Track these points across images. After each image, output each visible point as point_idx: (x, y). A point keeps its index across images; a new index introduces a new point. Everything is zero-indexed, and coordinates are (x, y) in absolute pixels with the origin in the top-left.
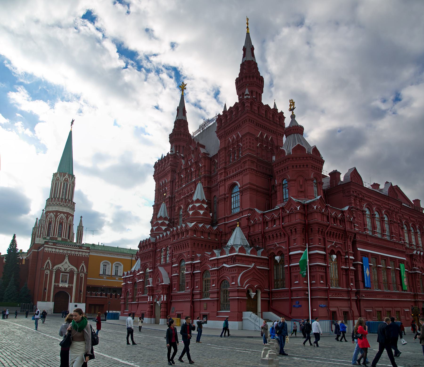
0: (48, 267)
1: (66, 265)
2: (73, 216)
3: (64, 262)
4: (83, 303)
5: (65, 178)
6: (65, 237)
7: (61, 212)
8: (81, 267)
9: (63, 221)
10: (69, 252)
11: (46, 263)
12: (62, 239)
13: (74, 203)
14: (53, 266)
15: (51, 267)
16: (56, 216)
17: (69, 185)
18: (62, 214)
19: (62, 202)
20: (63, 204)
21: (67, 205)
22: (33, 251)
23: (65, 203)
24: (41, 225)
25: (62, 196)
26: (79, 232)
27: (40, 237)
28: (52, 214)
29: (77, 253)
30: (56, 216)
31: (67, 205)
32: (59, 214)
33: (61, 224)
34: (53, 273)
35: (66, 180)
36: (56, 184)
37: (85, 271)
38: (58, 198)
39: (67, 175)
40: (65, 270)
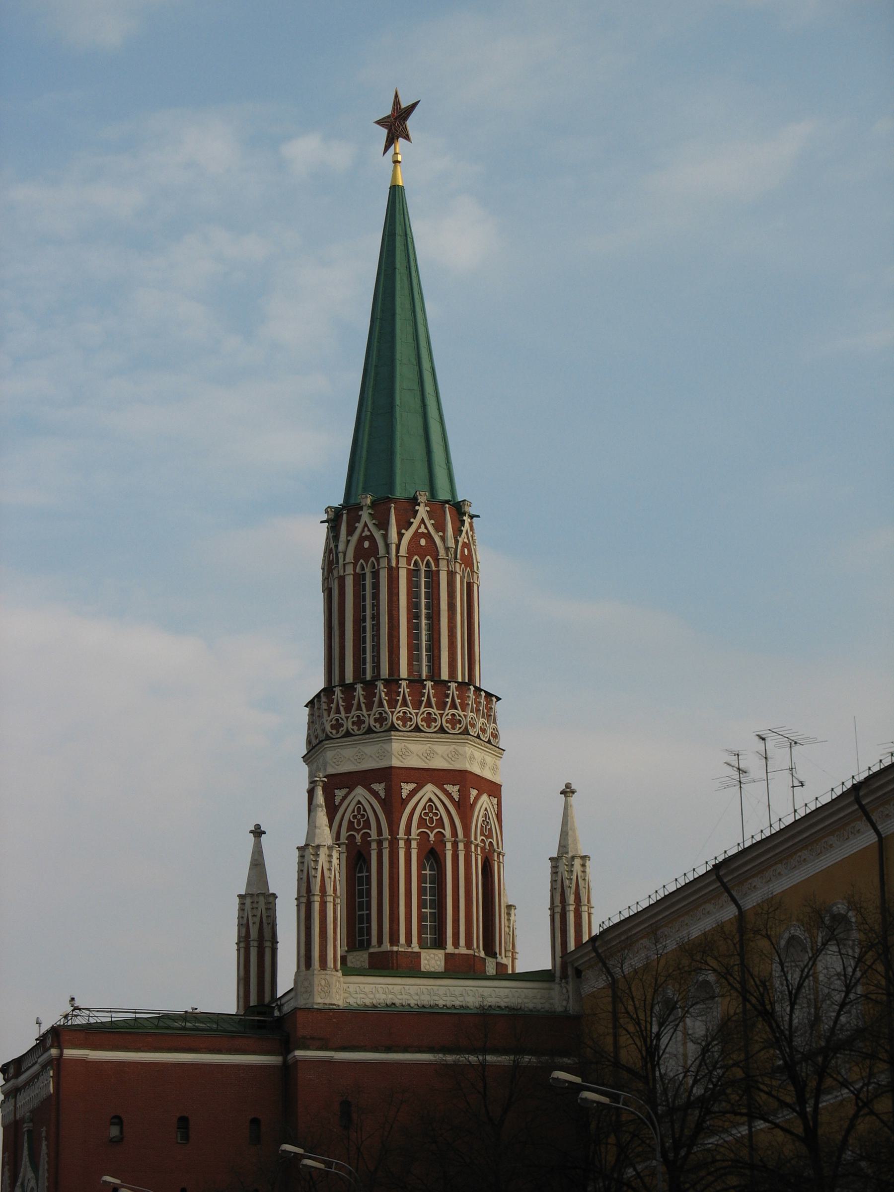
2: (494, 790)
5: (417, 535)
6: (469, 945)
12: (448, 957)
13: (489, 695)
17: (443, 576)
18: (429, 790)
19: (417, 705)
20: (429, 719)
21: (454, 721)
23: (442, 706)
25: (414, 658)
28: (360, 793)
30: (392, 805)
31: (454, 721)
32: (407, 788)
33: (432, 856)
35: (422, 548)
36: (359, 579)
38: (393, 682)
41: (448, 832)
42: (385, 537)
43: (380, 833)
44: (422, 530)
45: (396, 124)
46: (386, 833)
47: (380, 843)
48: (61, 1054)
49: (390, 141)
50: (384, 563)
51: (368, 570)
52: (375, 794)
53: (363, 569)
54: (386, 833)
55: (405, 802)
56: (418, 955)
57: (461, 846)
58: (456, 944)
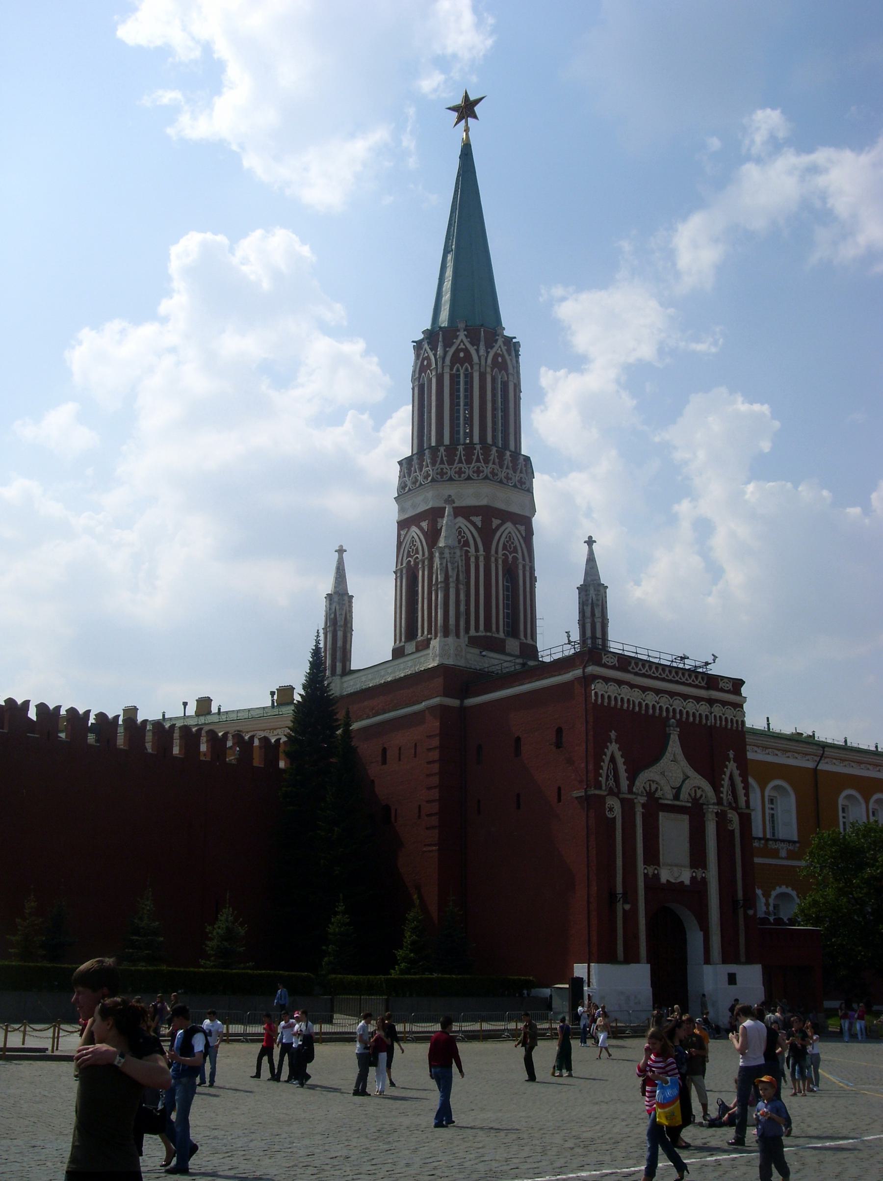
0: (611, 782)
1: (672, 772)
3: (668, 755)
4: (749, 961)
5: (496, 355)
7: (506, 516)
8: (726, 778)
9: (515, 559)
10: (678, 704)
11: (607, 759)
14: (632, 779)
15: (624, 783)
16: (487, 534)
18: (509, 525)
21: (522, 482)
22: (442, 708)
24: (452, 574)
25: (494, 437)
27: (458, 635)
29: (703, 709)
30: (487, 534)
32: (496, 522)
34: (634, 814)
36: (454, 379)
37: (742, 800)
38: (486, 449)
39: (500, 342)
40: (677, 797)
41: (520, 556)
42: (477, 351)
43: (477, 550)
44: (499, 351)
45: (466, 109)
46: (481, 552)
49: (459, 120)
50: (476, 367)
51: (462, 372)
52: (474, 524)
53: (458, 370)
56: (503, 641)
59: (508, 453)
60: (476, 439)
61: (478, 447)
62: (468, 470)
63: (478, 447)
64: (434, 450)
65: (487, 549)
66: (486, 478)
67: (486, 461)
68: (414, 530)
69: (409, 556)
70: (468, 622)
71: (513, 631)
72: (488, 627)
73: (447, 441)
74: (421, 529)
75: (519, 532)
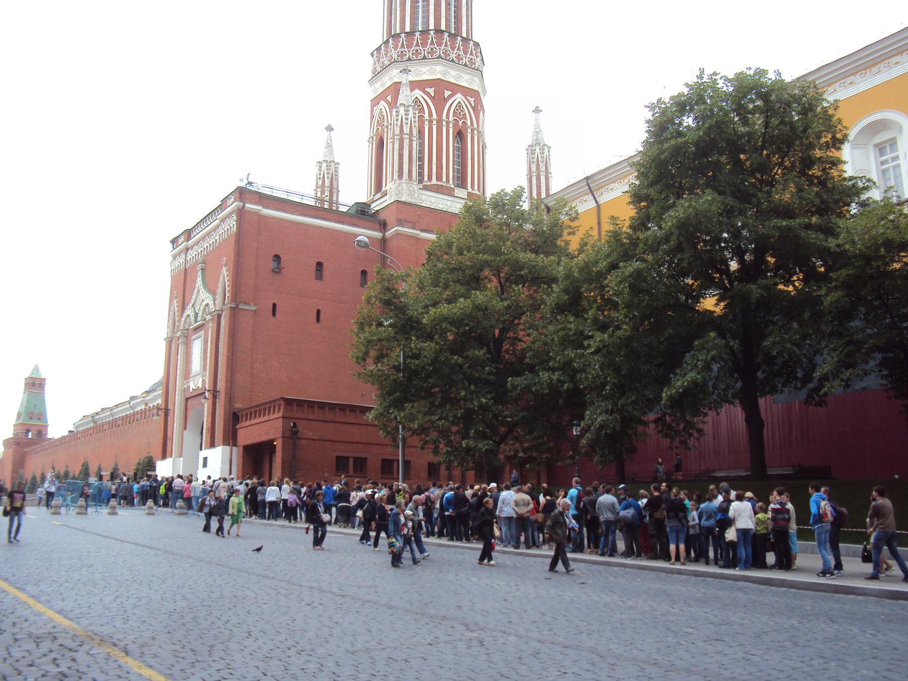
7: (456, 88)
16: (439, 101)
18: (459, 97)
26: (534, 168)
28: (418, 93)
30: (439, 101)
32: (447, 93)
43: (430, 114)
46: (435, 116)
47: (430, 122)
48: (244, 206)
52: (428, 94)
54: (435, 116)
55: (446, 100)
57: (476, 132)
58: (473, 187)
59: (459, 38)
60: (432, 26)
61: (432, 32)
62: (424, 51)
63: (432, 32)
64: (397, 36)
65: (440, 114)
66: (440, 57)
67: (439, 44)
68: (382, 103)
69: (378, 124)
70: (421, 174)
71: (462, 183)
72: (439, 178)
73: (408, 29)
74: (387, 102)
75: (469, 102)
